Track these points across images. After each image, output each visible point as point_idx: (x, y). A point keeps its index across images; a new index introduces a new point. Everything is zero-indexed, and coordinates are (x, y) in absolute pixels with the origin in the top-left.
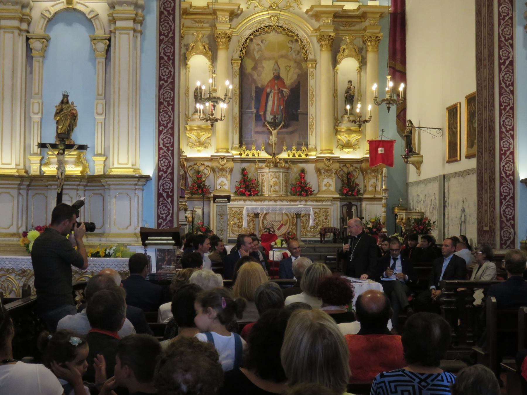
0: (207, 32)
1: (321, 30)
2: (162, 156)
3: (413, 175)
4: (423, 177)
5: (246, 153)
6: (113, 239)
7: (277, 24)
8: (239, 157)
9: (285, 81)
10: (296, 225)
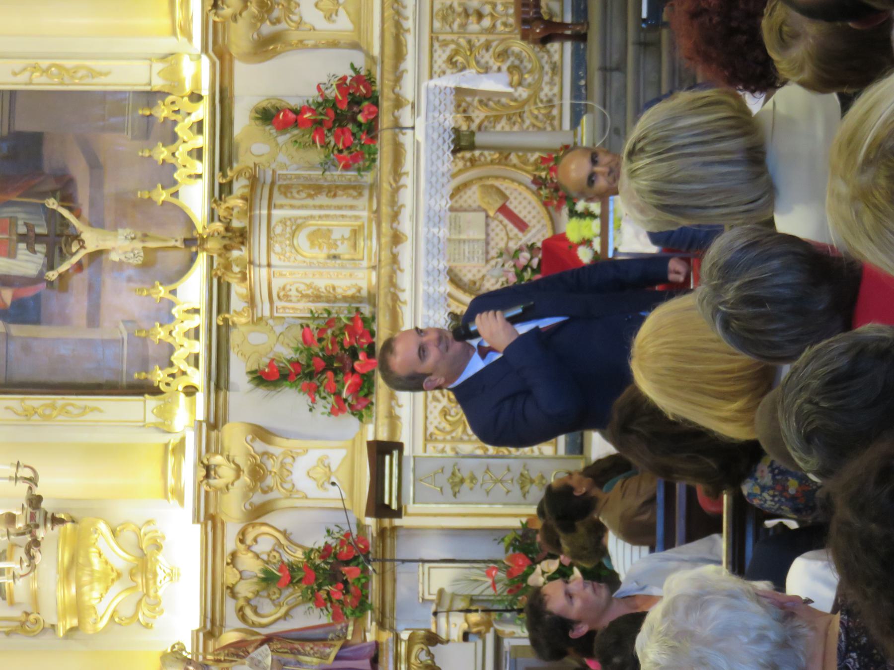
5: (184, 366)
8: (200, 397)
10: (504, 152)
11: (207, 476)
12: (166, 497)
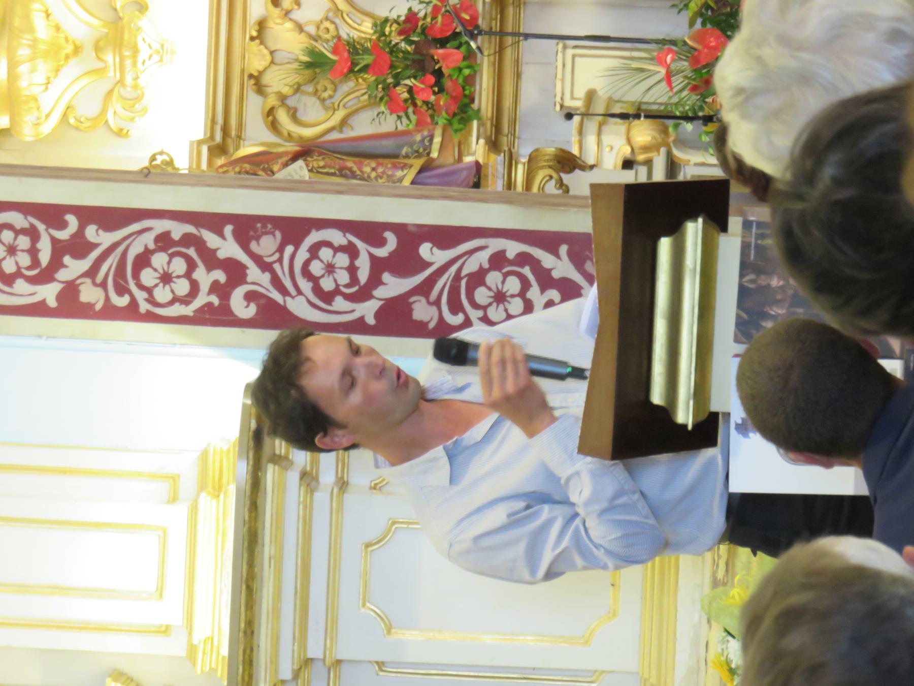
2: (122, 290)
6: (683, 656)
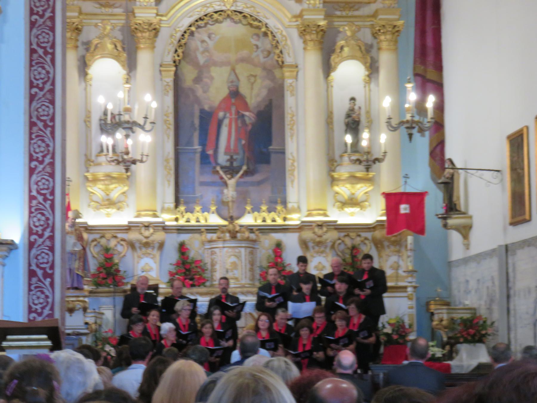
0: (120, 21)
1: (305, 17)
2: (36, 210)
3: (457, 251)
4: (474, 250)
7: (233, 8)
8: (175, 223)
9: (248, 100)
11: (146, 226)
12: (138, 211)
